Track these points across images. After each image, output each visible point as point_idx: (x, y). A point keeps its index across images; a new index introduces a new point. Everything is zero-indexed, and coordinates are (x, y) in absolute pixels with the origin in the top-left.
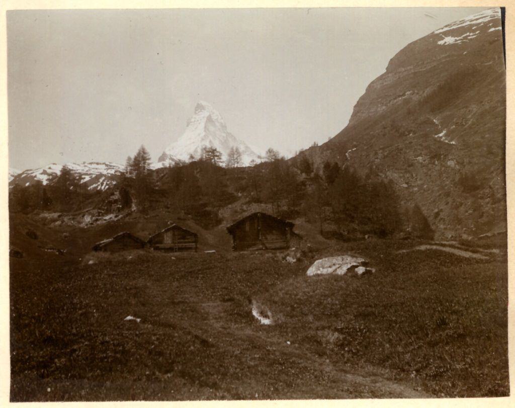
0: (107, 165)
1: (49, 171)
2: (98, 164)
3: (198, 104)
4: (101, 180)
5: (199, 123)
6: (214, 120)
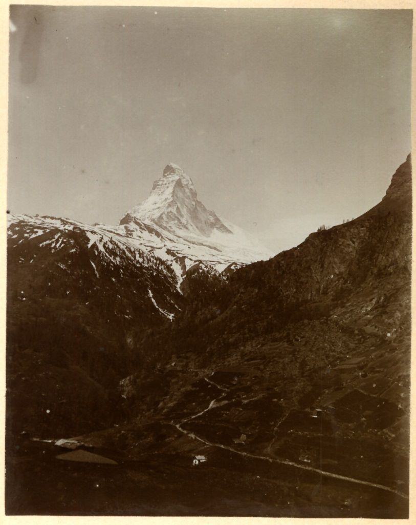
0: (62, 221)
2: (52, 218)
3: (168, 167)
4: (56, 237)
5: (168, 187)
6: (183, 185)
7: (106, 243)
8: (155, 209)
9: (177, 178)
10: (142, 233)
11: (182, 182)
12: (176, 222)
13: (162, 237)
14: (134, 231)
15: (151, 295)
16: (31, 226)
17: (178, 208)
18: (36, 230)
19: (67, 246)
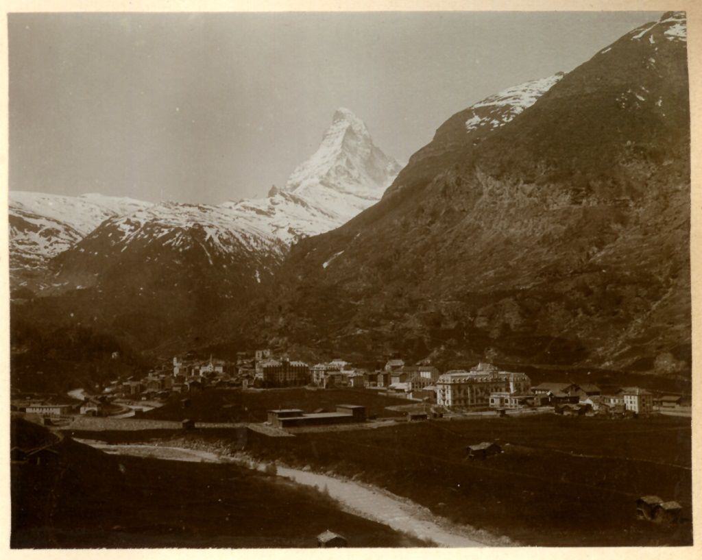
0: (200, 208)
1: (133, 220)
2: (190, 206)
3: (337, 112)
4: (177, 235)
5: (337, 137)
6: (355, 132)
7: (221, 235)
10: (287, 204)
11: (353, 128)
12: (346, 176)
13: (308, 206)
14: (277, 204)
15: (258, 275)
16: (160, 225)
17: (348, 161)
18: (162, 230)
19: (185, 243)
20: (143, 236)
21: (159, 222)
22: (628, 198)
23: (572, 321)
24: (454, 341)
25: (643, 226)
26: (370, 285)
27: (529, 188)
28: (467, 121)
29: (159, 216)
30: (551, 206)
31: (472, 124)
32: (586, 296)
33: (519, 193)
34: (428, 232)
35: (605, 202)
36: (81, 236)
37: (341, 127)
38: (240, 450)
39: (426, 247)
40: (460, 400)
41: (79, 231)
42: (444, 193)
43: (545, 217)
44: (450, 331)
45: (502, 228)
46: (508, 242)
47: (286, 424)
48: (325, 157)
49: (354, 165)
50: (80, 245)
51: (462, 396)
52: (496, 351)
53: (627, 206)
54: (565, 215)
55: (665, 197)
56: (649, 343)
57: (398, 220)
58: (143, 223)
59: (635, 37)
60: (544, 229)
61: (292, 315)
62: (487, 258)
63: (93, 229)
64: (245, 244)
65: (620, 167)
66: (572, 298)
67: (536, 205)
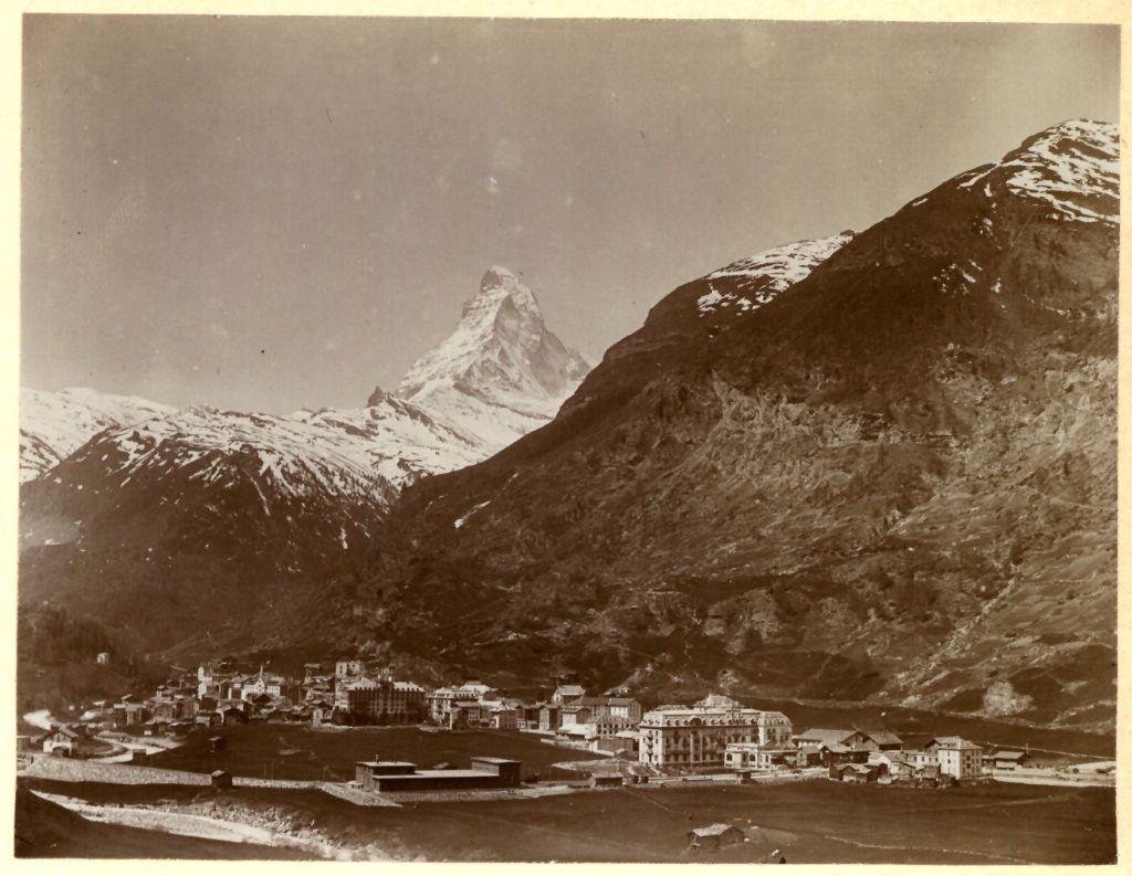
0: (253, 419)
1: (143, 434)
2: (238, 415)
4: (214, 463)
5: (487, 313)
6: (517, 306)
7: (286, 466)
8: (463, 356)
9: (503, 294)
10: (398, 419)
12: (499, 377)
13: (432, 425)
14: (383, 418)
15: (344, 536)
16: (186, 445)
17: (502, 353)
18: (190, 453)
19: (226, 476)
20: (157, 462)
21: (186, 439)
22: (948, 433)
23: (860, 628)
24: (668, 657)
25: (972, 478)
26: (532, 560)
27: (795, 410)
28: (699, 297)
29: (185, 430)
30: (830, 440)
31: (708, 303)
32: (883, 589)
33: (781, 417)
34: (630, 474)
35: (913, 438)
36: (57, 457)
37: (493, 298)
38: (308, 825)
39: (629, 500)
40: (676, 756)
41: (54, 449)
42: (659, 412)
43: (819, 457)
44: (663, 639)
45: (752, 473)
46: (760, 495)
47: (386, 786)
48: (465, 344)
49: (512, 360)
50: (56, 471)
51: (680, 748)
52: (736, 675)
53: (947, 445)
54: (851, 457)
55: (1005, 435)
56: (977, 666)
57: (583, 453)
58: (159, 440)
59: (964, 185)
60: (817, 477)
61: (400, 604)
62: (724, 521)
63: (78, 446)
64: (326, 483)
65: (937, 384)
66: (860, 591)
67: (806, 438)
